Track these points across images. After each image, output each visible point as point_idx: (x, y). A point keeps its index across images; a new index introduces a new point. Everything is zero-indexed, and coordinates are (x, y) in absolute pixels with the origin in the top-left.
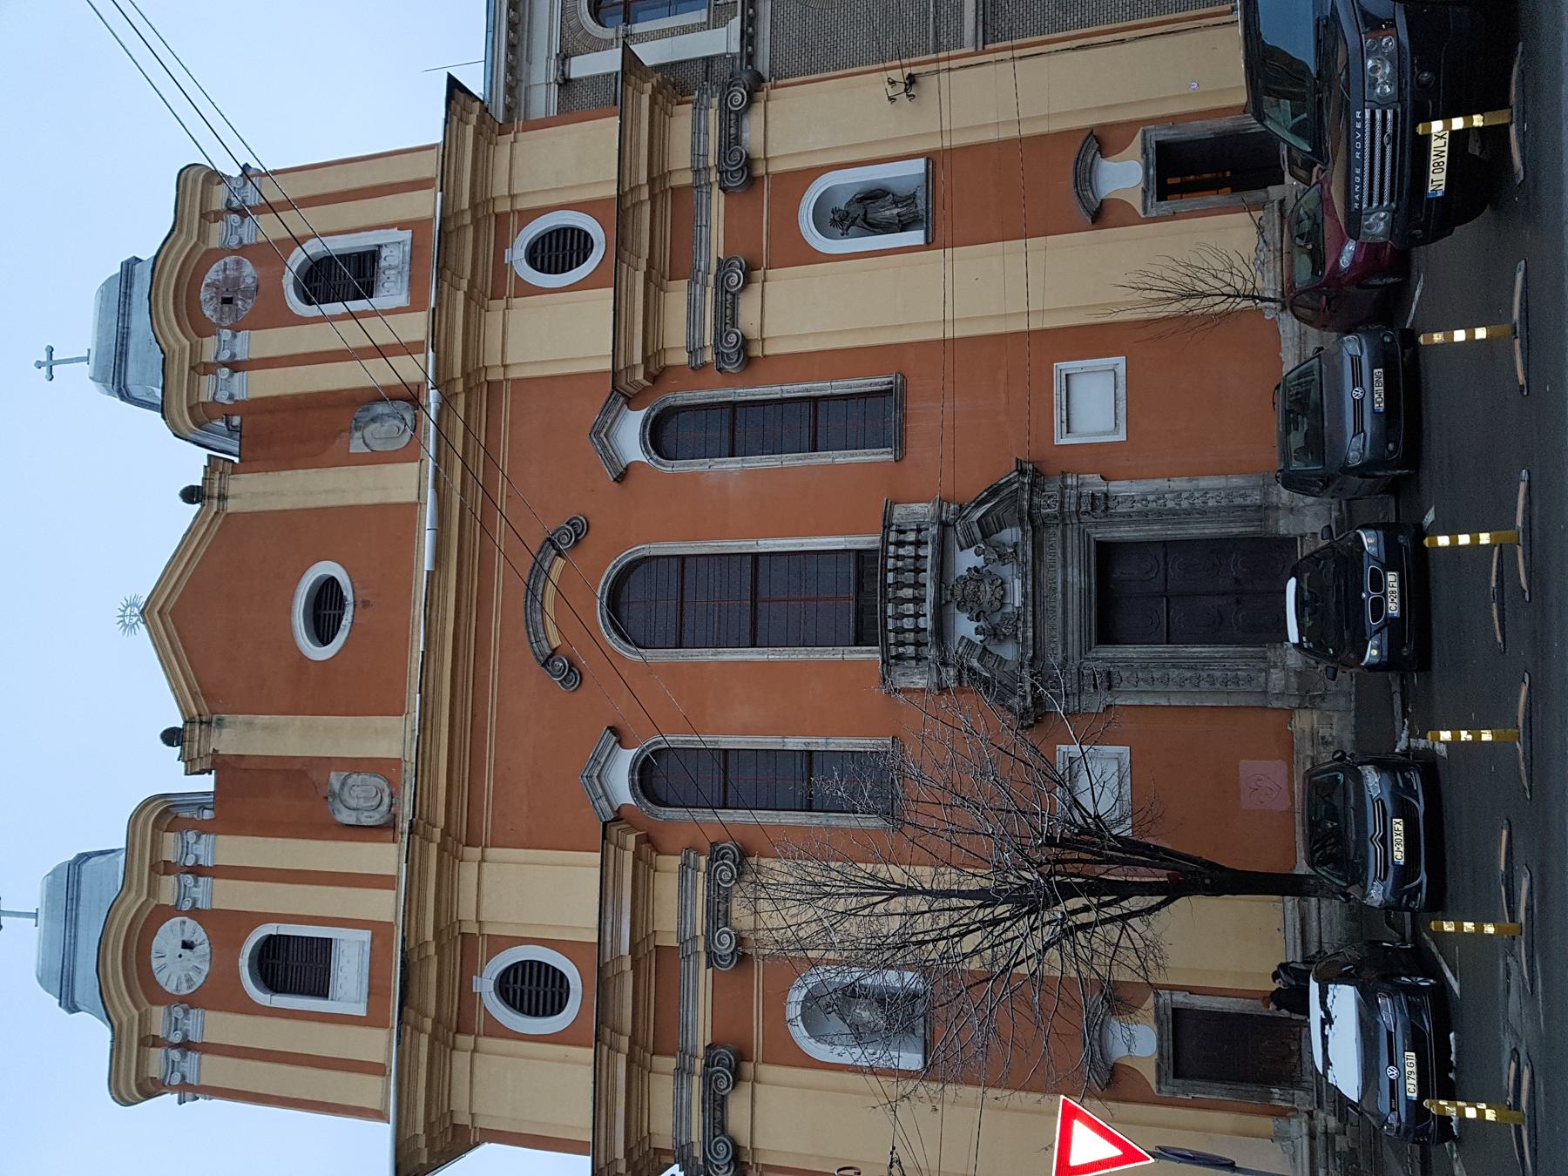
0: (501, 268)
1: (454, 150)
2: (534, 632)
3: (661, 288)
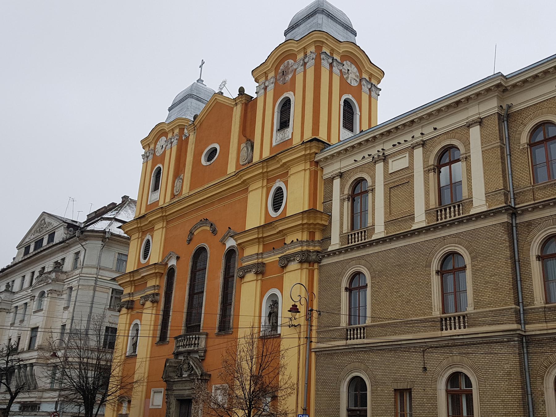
0: (274, 180)
1: (296, 150)
2: (195, 227)
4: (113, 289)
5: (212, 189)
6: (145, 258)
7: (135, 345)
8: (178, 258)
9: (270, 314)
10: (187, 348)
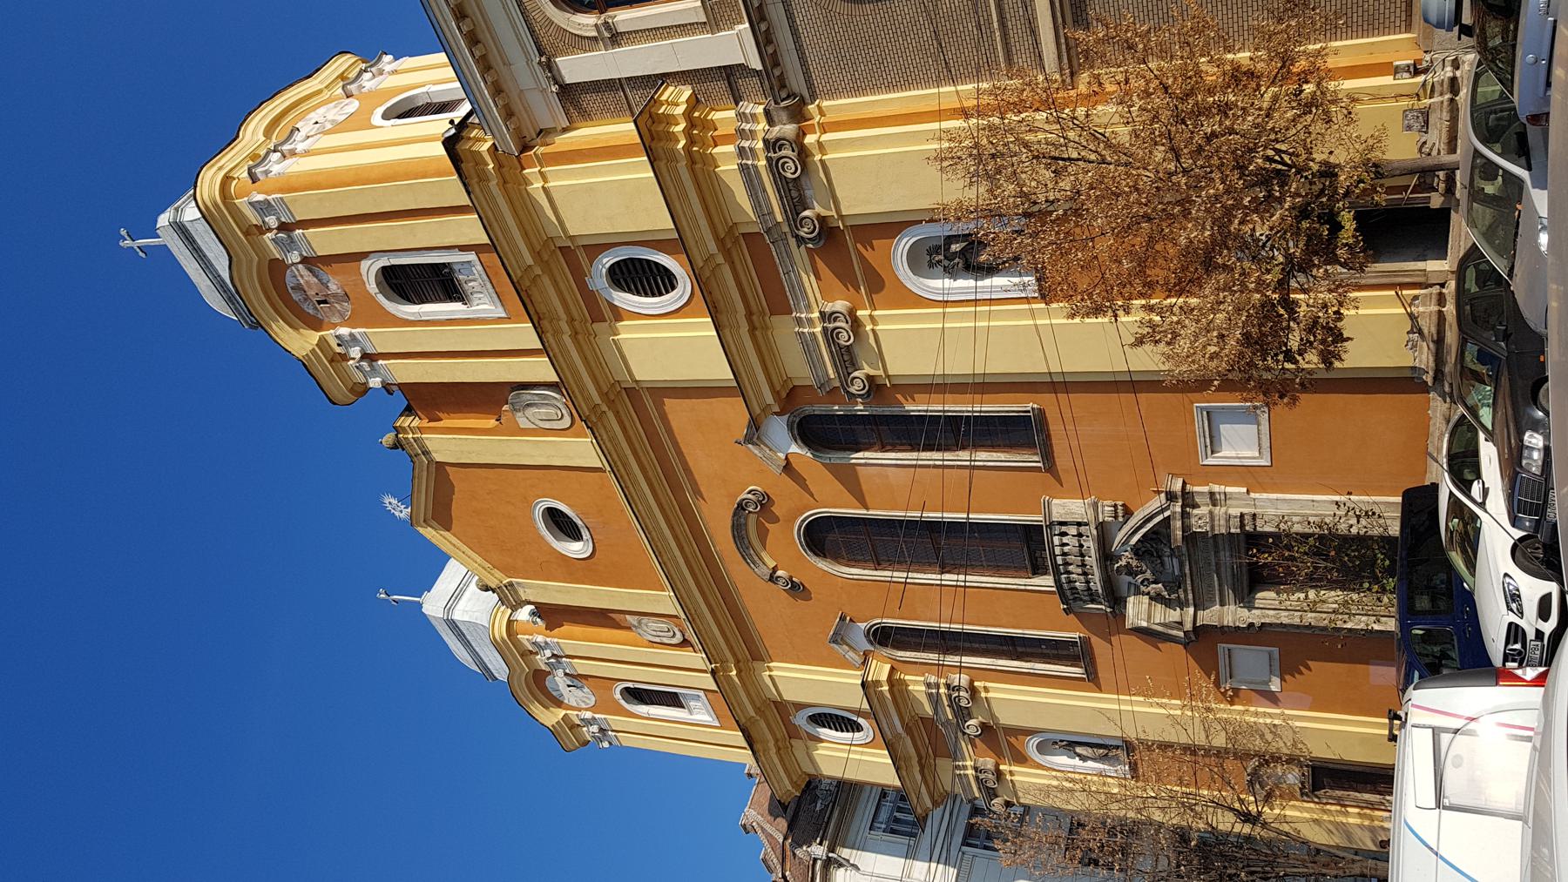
0: (590, 298)
1: (490, 214)
3: (766, 328)
4: (963, 844)
5: (641, 508)
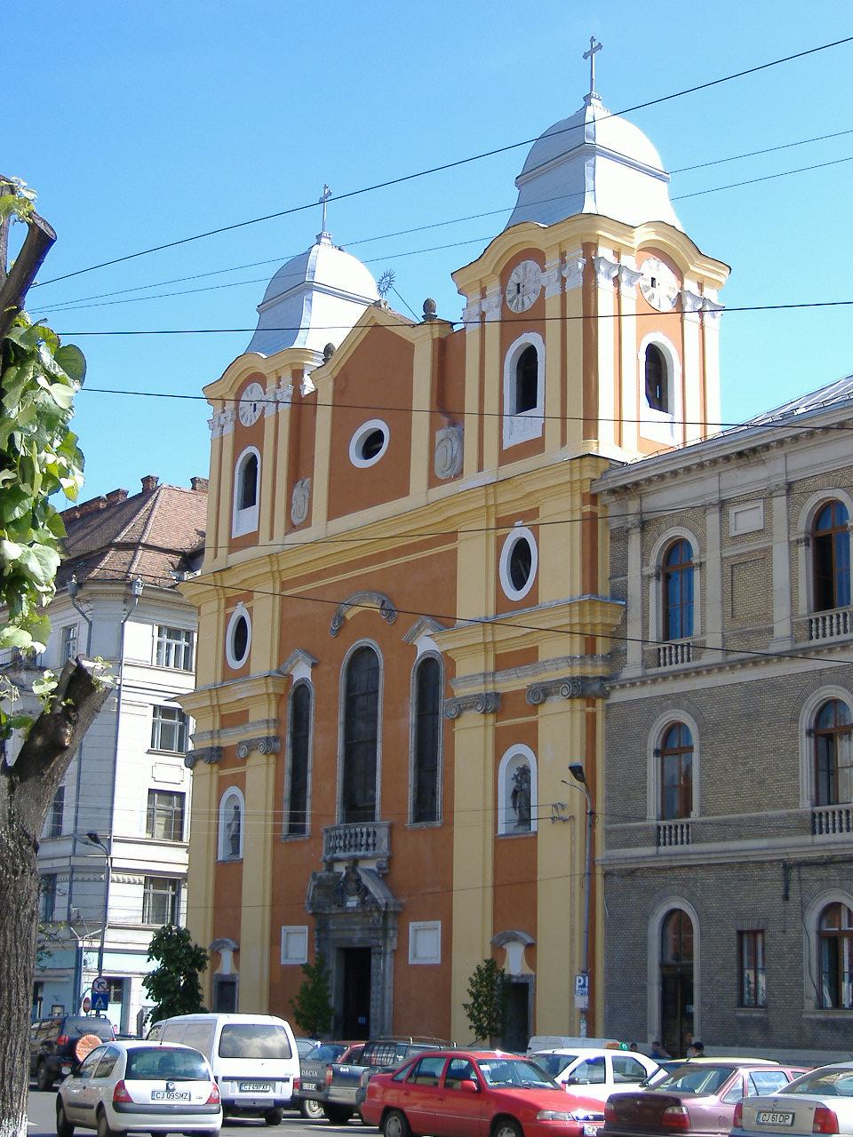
6: (239, 656)
7: (235, 840)
8: (314, 666)
9: (515, 793)
10: (353, 853)
